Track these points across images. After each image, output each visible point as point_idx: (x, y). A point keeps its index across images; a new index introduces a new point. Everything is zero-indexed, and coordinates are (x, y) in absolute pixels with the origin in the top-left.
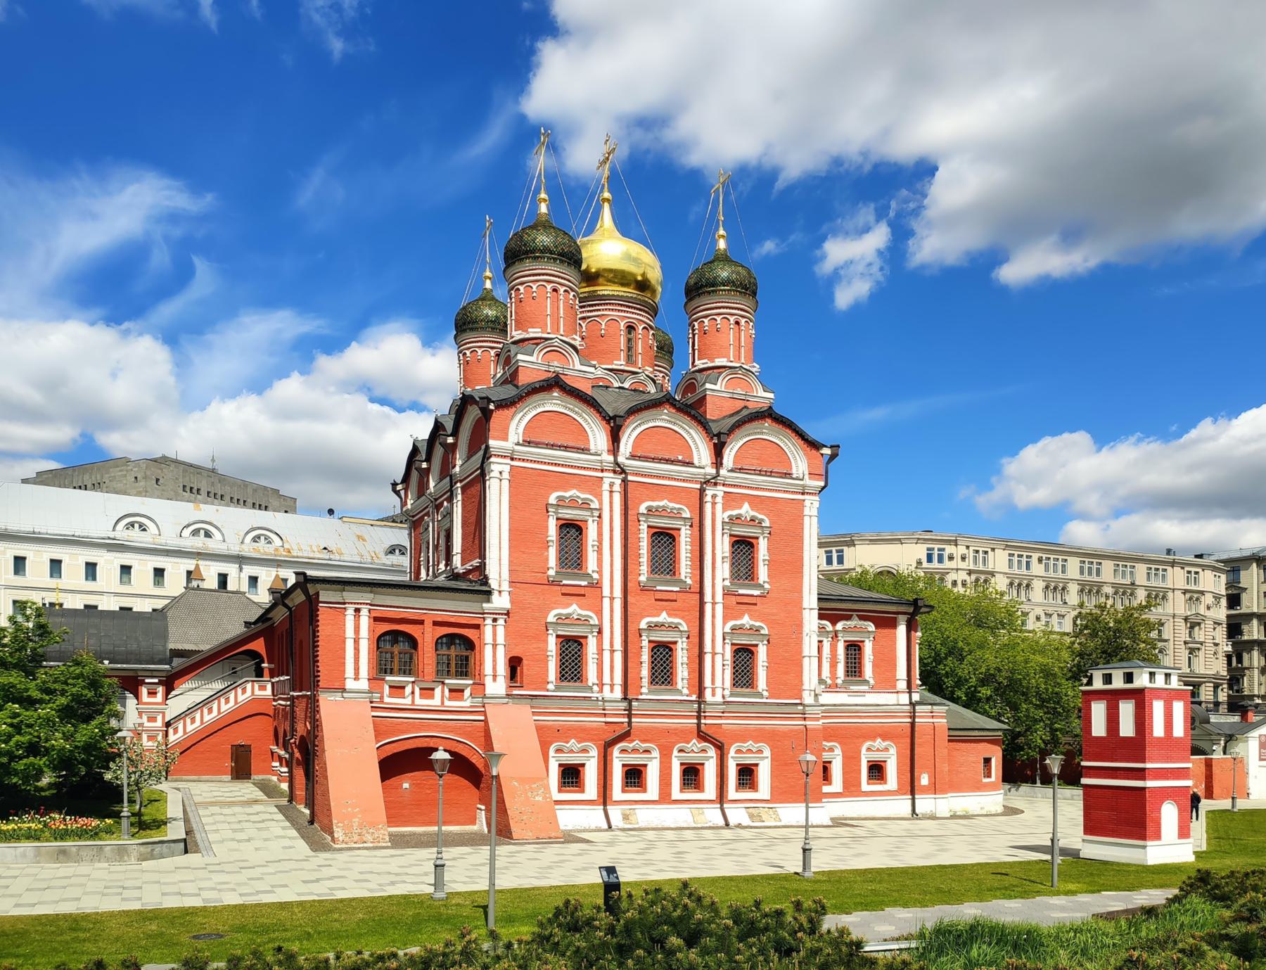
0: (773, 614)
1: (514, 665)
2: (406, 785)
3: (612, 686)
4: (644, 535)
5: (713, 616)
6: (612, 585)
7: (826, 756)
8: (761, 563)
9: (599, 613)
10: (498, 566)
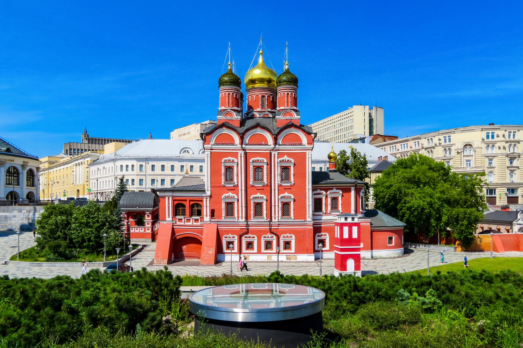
9: (238, 195)
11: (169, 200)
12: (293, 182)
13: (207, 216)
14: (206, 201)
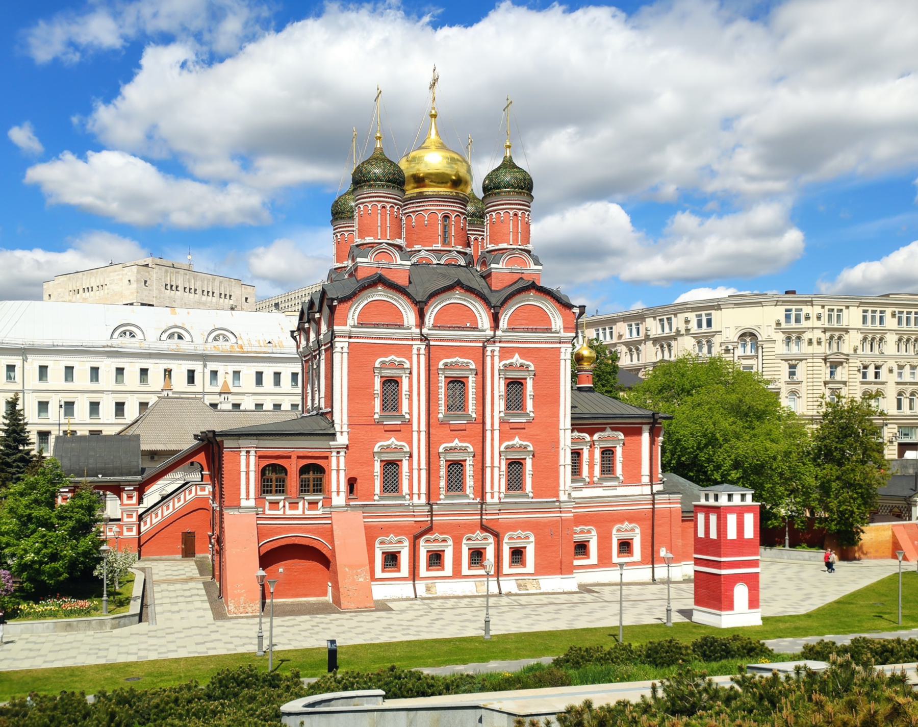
0: (537, 435)
1: (352, 483)
2: (281, 570)
3: (419, 495)
4: (442, 384)
5: (492, 439)
6: (419, 422)
7: (579, 537)
8: (528, 397)
9: (410, 444)
13: (338, 493)
14: (338, 458)
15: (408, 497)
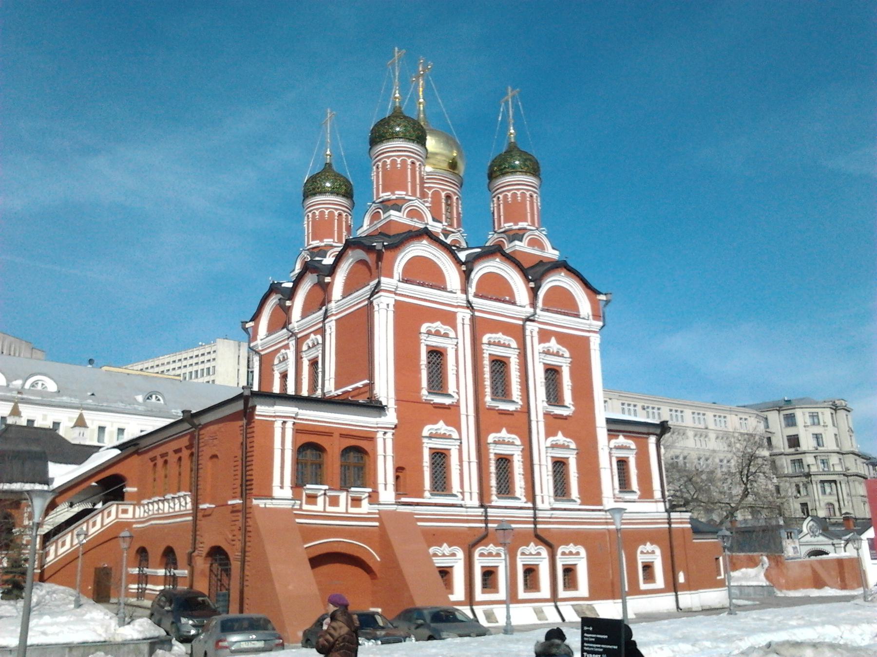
4: (486, 362)
10: (385, 388)
11: (283, 429)
12: (573, 408)
15: (460, 496)
